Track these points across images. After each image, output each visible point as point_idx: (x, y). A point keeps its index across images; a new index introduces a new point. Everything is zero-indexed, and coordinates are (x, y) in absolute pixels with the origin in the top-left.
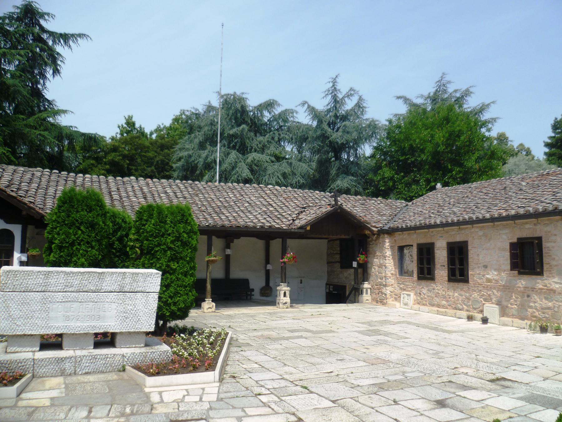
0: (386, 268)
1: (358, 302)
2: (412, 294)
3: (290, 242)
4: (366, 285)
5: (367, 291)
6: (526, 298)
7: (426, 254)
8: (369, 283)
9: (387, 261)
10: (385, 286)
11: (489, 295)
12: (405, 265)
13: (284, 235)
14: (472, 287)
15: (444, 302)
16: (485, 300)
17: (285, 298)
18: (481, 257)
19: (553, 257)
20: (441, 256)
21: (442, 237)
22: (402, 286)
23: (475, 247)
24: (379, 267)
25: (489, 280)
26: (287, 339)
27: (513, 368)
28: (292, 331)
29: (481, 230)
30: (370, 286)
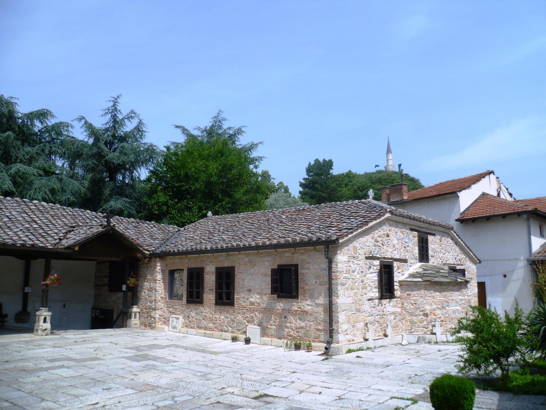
0: (156, 291)
1: (126, 327)
2: (181, 317)
3: (55, 263)
4: (135, 309)
5: (135, 315)
6: (283, 319)
7: (195, 279)
8: (138, 307)
9: (158, 285)
10: (155, 309)
11: (252, 317)
12: (175, 288)
13: (48, 255)
14: (237, 309)
15: (211, 325)
16: (248, 322)
17: (45, 324)
18: (246, 281)
19: (307, 282)
20: (210, 280)
21: (211, 262)
22: (171, 310)
24: (149, 291)
25: (252, 303)
26: (46, 369)
27: (274, 384)
28: (52, 361)
29: (246, 257)
30: (138, 310)
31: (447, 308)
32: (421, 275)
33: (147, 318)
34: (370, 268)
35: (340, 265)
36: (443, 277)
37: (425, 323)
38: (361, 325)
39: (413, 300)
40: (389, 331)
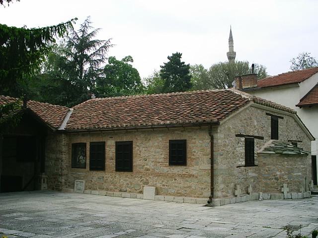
0: (62, 161)
4: (44, 176)
5: (44, 180)
8: (46, 174)
9: (64, 156)
10: (61, 175)
15: (112, 187)
20: (111, 151)
21: (112, 137)
25: (148, 170)
31: (292, 174)
32: (274, 149)
33: (54, 182)
34: (239, 143)
35: (219, 141)
36: (290, 150)
37: (276, 185)
38: (232, 185)
39: (268, 168)
40: (250, 190)
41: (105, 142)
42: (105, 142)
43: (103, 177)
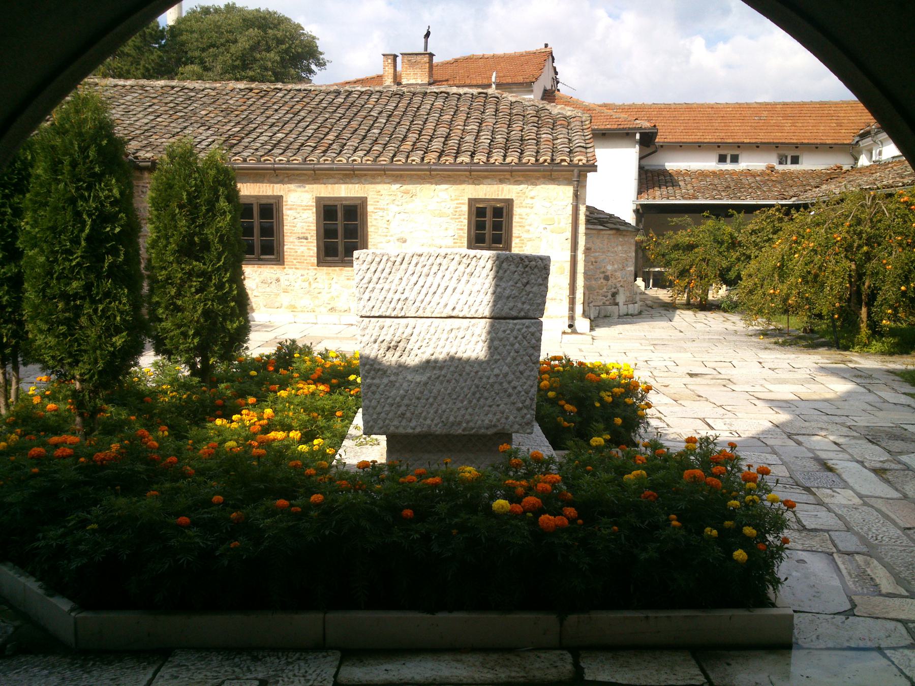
19: (527, 228)
23: (383, 209)
37: (605, 290)
41: (282, 196)
42: (279, 199)
43: (278, 280)
